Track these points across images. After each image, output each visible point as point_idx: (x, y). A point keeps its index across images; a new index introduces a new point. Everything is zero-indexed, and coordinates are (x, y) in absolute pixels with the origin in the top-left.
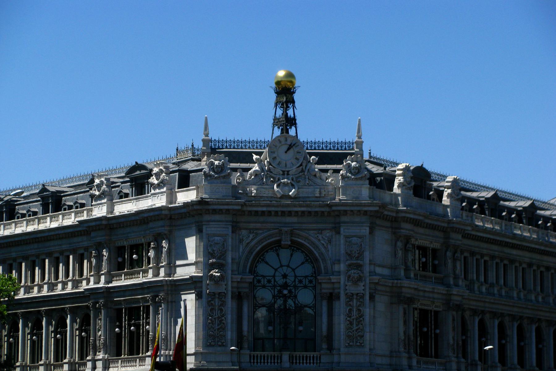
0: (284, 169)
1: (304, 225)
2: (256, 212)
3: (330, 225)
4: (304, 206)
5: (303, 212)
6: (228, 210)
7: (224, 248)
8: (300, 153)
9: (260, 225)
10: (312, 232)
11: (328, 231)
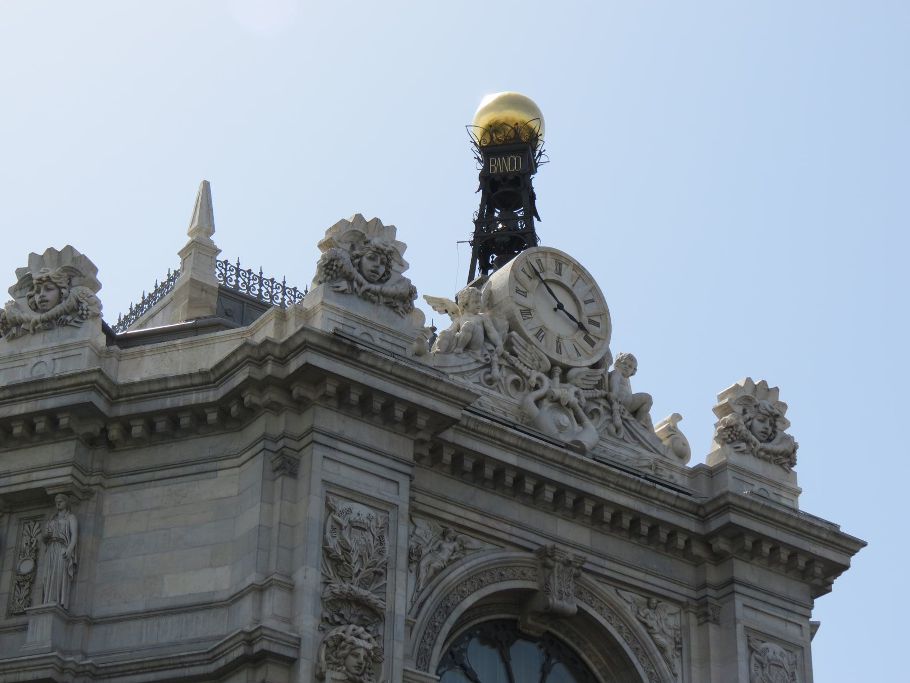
0: (556, 357)
1: (608, 564)
2: (481, 460)
3: (684, 591)
4: (629, 492)
5: (619, 511)
6: (413, 410)
7: (381, 553)
8: (598, 325)
9: (476, 517)
10: (627, 595)
11: (673, 608)
